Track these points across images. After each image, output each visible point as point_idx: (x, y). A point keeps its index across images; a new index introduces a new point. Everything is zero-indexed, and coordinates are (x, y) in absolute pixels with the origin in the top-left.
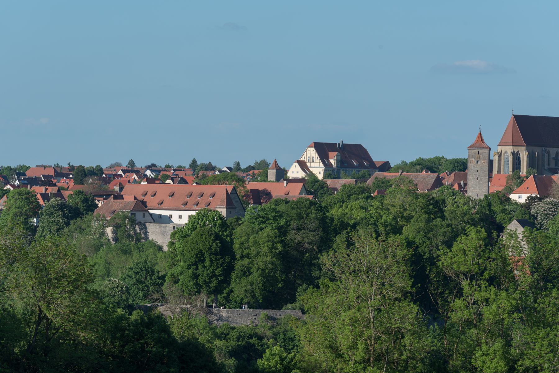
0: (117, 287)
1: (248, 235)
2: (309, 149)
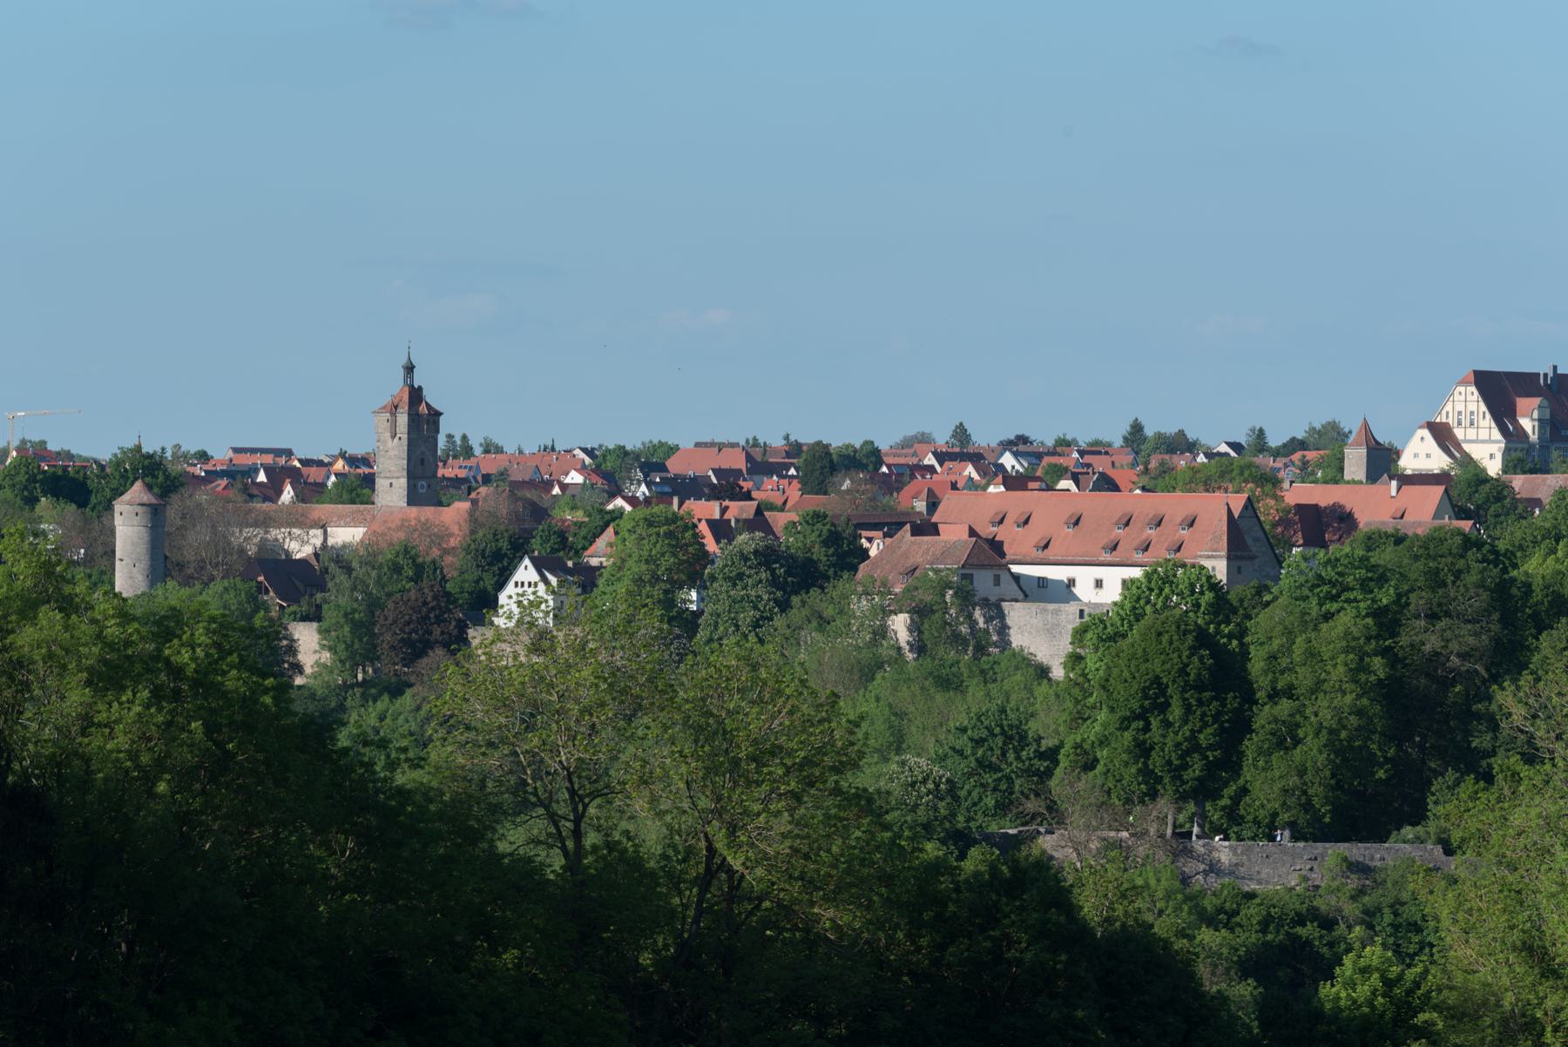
0: (924, 781)
1: (1289, 633)
2: (1462, 389)
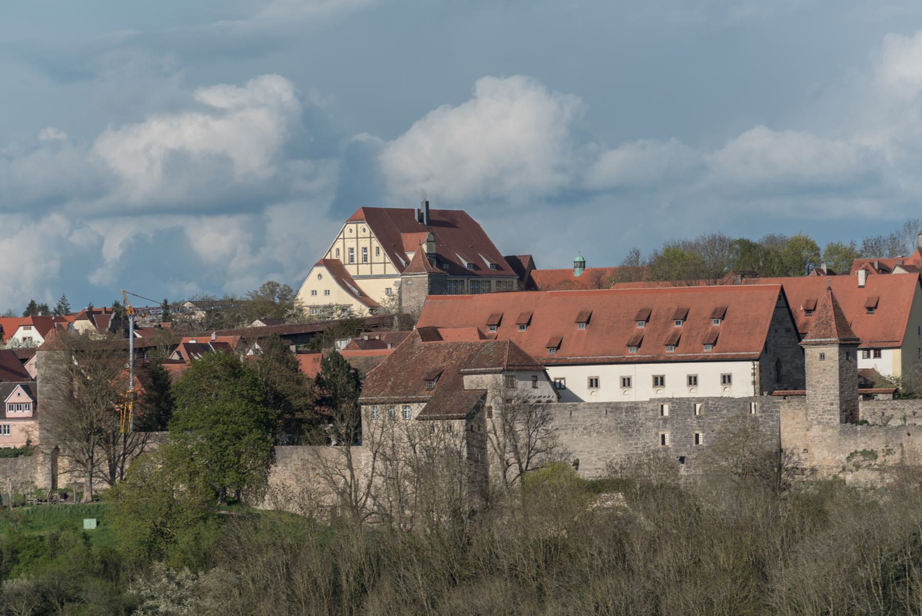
2: (353, 226)
